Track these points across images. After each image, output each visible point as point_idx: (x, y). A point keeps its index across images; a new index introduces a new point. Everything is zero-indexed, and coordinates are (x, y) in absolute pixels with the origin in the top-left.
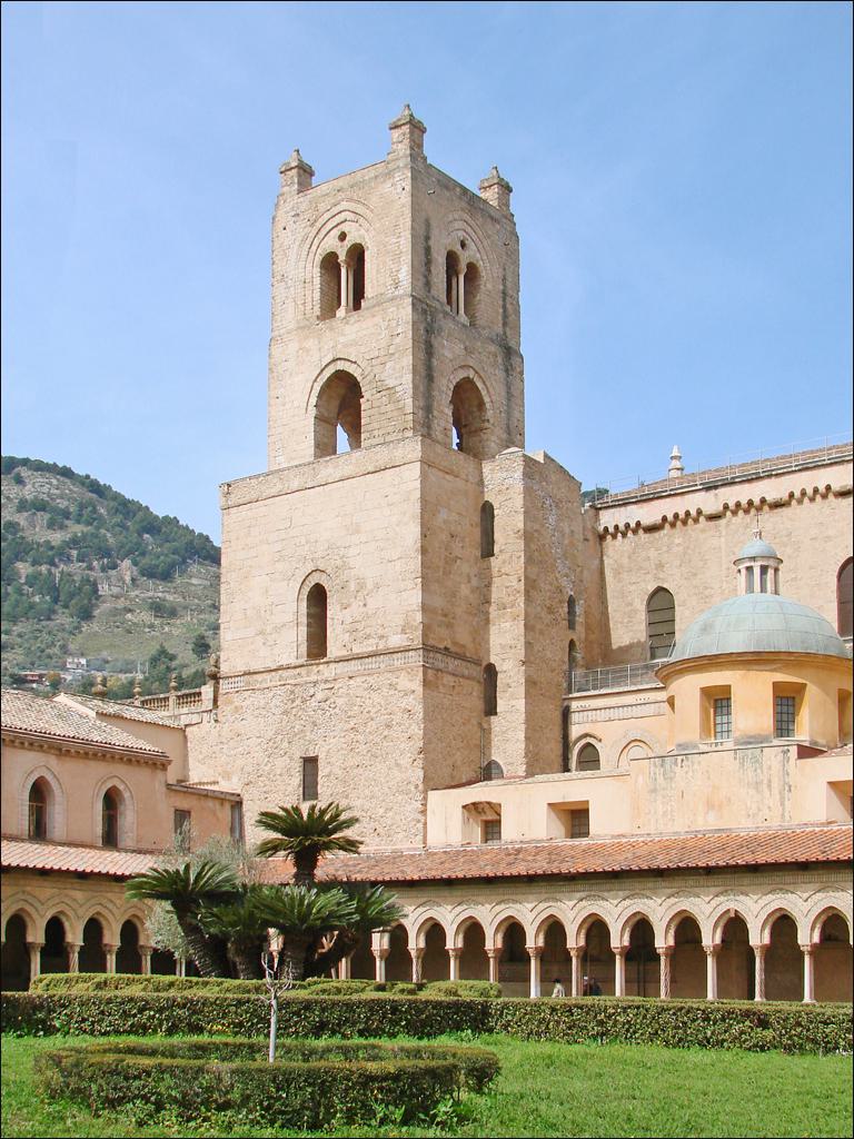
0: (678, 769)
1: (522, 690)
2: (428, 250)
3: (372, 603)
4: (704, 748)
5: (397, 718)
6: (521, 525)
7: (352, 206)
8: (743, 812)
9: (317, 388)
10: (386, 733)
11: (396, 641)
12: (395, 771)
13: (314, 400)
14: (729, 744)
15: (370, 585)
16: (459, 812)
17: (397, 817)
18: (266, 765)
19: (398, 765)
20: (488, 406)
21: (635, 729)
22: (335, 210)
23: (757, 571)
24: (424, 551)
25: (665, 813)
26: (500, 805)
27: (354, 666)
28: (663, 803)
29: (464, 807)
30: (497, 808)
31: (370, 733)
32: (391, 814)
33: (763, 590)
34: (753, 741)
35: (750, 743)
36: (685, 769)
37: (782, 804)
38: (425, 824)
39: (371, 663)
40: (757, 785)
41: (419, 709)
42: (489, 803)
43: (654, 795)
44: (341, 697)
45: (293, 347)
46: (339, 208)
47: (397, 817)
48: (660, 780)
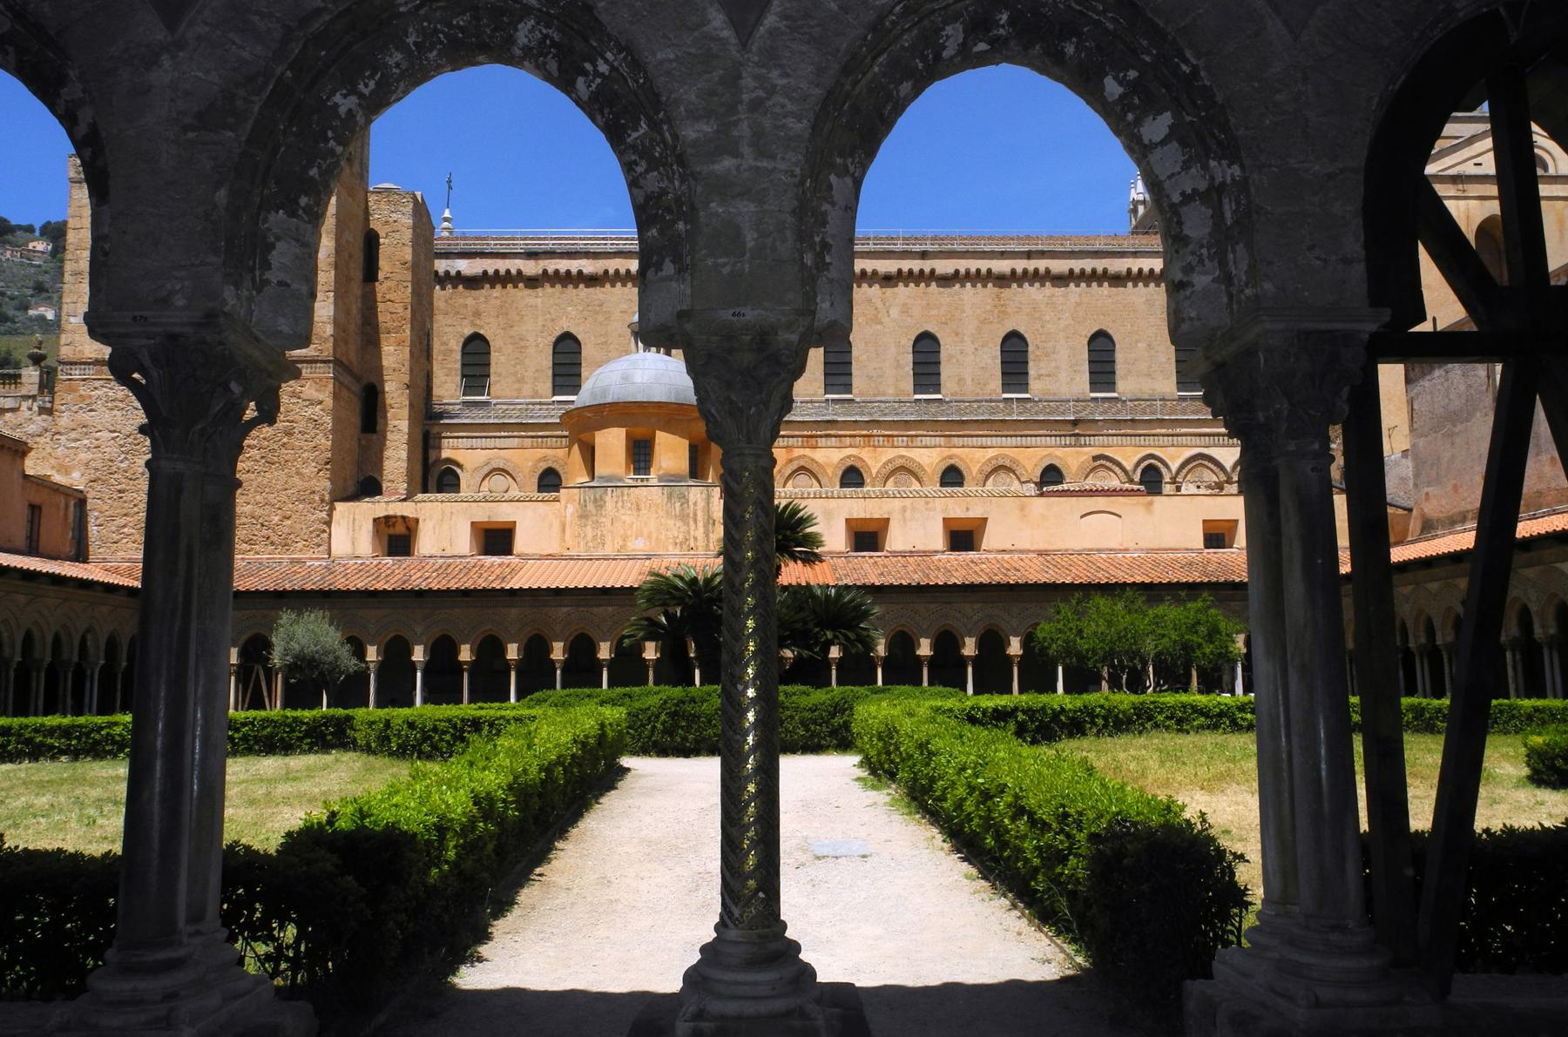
1: (405, 412)
4: (631, 483)
5: (299, 427)
6: (409, 257)
8: (671, 541)
10: (285, 440)
12: (296, 479)
14: (654, 482)
16: (368, 527)
17: (298, 526)
18: (122, 462)
19: (298, 473)
21: (499, 458)
24: (336, 268)
25: (595, 537)
26: (417, 521)
29: (375, 520)
30: (412, 525)
31: (264, 439)
32: (289, 522)
34: (669, 480)
35: (672, 481)
37: (707, 535)
38: (330, 534)
40: (683, 517)
41: (328, 419)
42: (404, 518)
43: (584, 520)
47: (298, 526)
48: (591, 507)
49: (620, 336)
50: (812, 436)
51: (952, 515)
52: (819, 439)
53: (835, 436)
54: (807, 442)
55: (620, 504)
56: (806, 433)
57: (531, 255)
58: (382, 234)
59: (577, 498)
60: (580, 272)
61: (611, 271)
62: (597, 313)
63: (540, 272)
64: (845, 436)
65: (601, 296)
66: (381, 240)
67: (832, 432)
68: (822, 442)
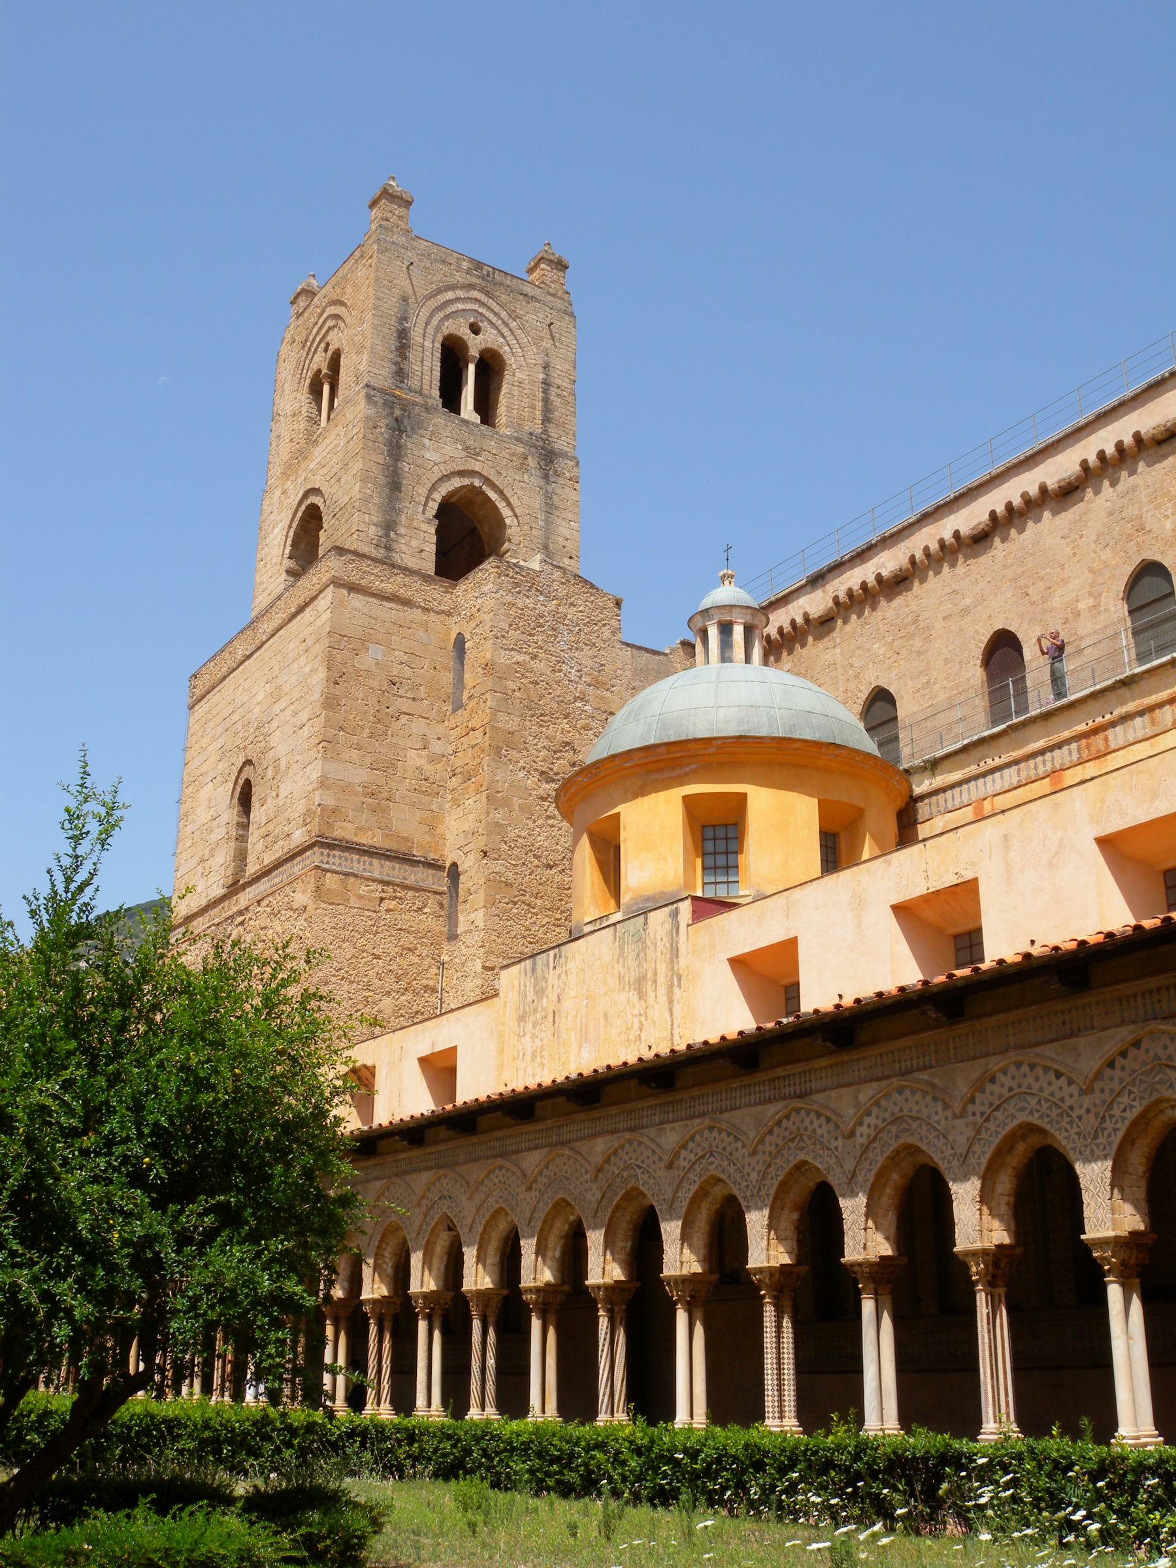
0: (552, 976)
2: (403, 335)
3: (284, 790)
7: (332, 310)
9: (291, 534)
11: (299, 837)
13: (287, 551)
15: (283, 768)
20: (508, 521)
22: (321, 321)
23: (738, 631)
24: (330, 702)
27: (263, 886)
28: (534, 1036)
33: (748, 660)
36: (558, 971)
39: (277, 878)
44: (250, 932)
45: (278, 492)
46: (325, 315)
49: (946, 661)
50: (1095, 731)
51: (1115, 824)
52: (1110, 733)
53: (1141, 713)
54: (1088, 747)
55: (563, 977)
56: (1082, 727)
57: (817, 580)
58: (467, 636)
59: (516, 983)
60: (879, 578)
61: (919, 555)
62: (911, 636)
63: (831, 603)
64: (1160, 705)
65: (914, 606)
66: (467, 645)
67: (1131, 707)
68: (1117, 736)
